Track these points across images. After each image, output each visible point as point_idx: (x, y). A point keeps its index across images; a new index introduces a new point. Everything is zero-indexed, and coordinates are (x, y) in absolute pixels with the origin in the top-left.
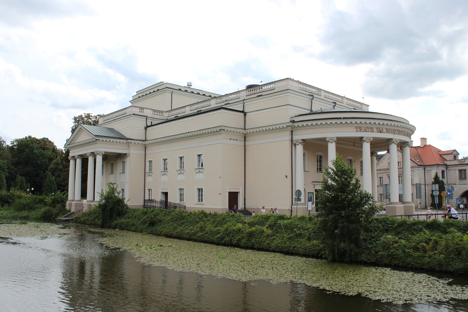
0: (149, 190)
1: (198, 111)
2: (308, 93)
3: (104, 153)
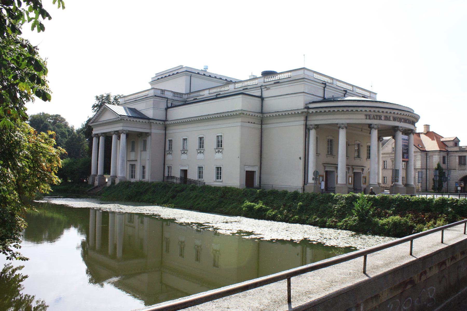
0: (169, 167)
1: (217, 95)
2: (321, 82)
3: (127, 132)
